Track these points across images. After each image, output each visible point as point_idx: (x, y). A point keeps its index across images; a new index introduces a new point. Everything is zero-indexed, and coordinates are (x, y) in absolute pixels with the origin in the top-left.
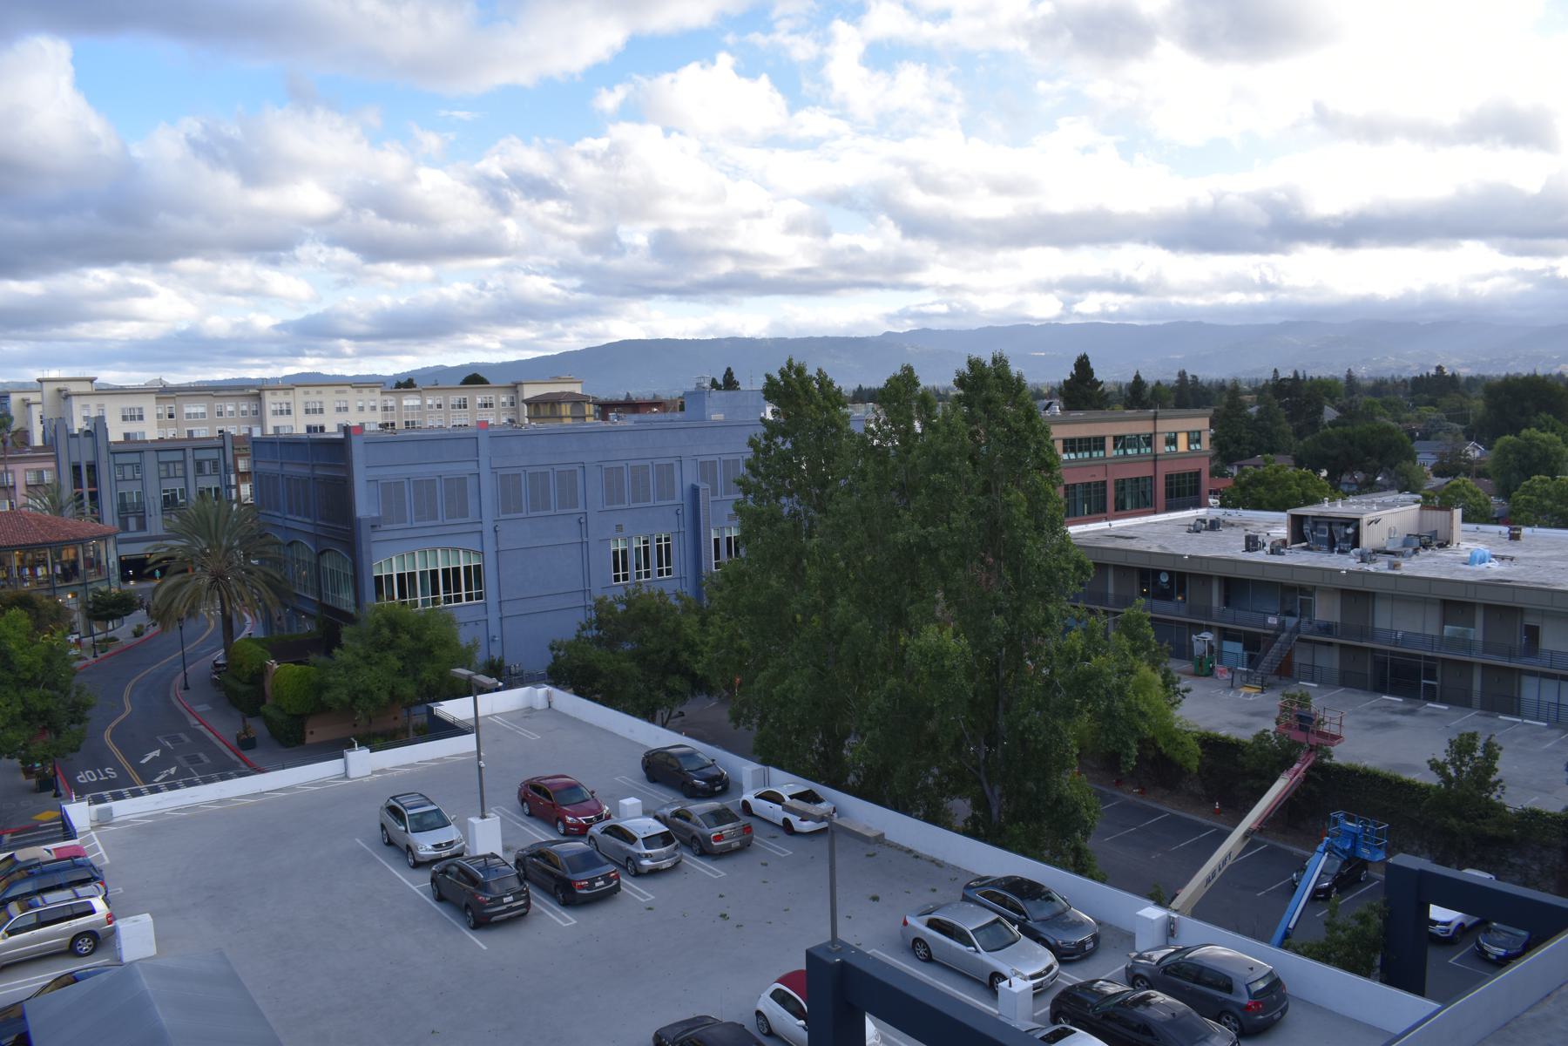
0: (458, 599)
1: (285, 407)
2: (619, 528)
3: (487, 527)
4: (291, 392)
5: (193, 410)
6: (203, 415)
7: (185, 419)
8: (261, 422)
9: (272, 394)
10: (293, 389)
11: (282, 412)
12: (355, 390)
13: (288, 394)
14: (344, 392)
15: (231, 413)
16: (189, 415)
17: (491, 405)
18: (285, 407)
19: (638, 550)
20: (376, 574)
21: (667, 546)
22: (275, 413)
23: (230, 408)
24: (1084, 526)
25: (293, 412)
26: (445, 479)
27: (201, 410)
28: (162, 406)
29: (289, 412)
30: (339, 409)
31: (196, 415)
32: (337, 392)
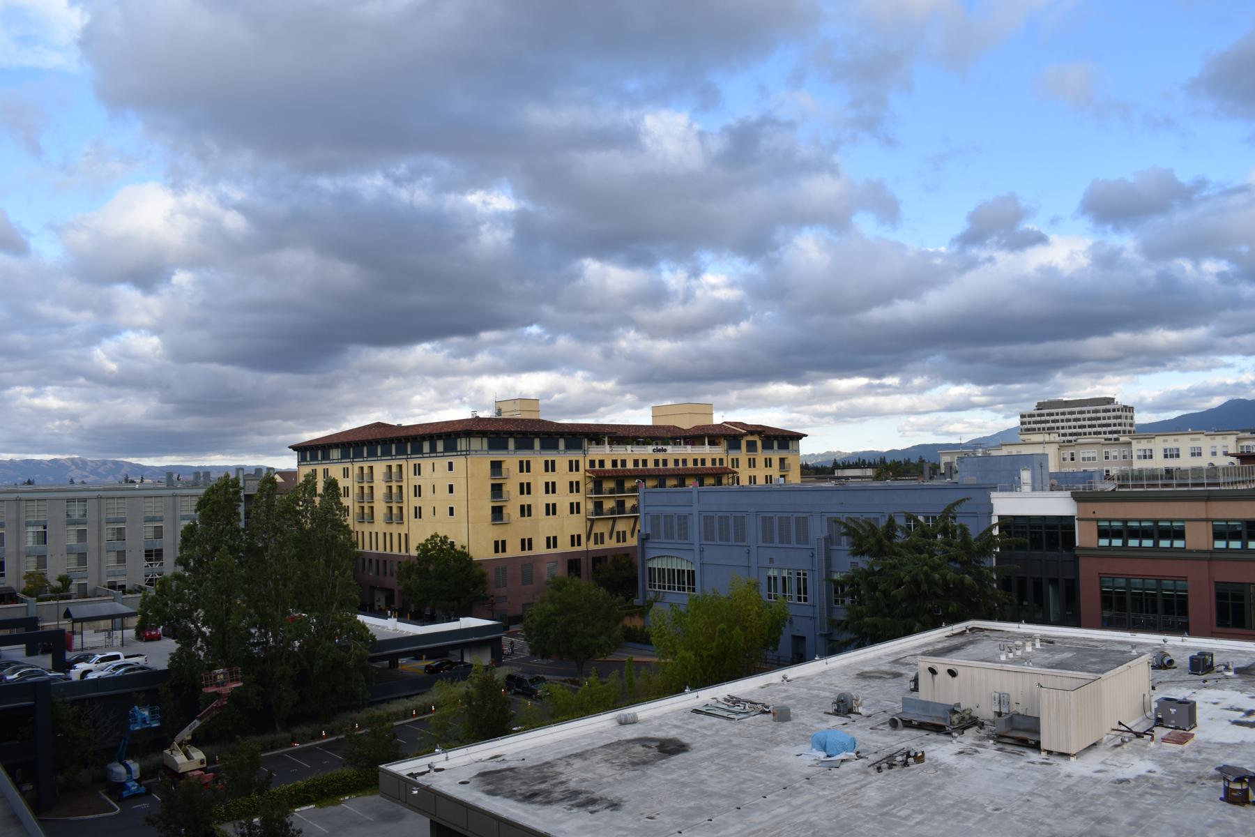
0: (684, 590)
1: (1148, 453)
2: (771, 560)
3: (696, 547)
4: (1153, 440)
5: (1087, 455)
6: (1094, 459)
7: (1081, 461)
8: (1131, 464)
9: (1138, 442)
10: (1154, 438)
11: (1145, 457)
12: (1209, 438)
13: (1151, 442)
14: (1199, 439)
15: (1115, 457)
16: (1084, 459)
17: (1200, 454)
18: (1148, 453)
19: (784, 579)
20: (650, 566)
21: (805, 580)
22: (1139, 457)
23: (1115, 454)
24: (1128, 634)
25: (1154, 456)
26: (678, 516)
27: (1091, 455)
28: (1066, 452)
29: (1151, 457)
30: (1193, 455)
31: (1089, 459)
32: (1192, 440)
